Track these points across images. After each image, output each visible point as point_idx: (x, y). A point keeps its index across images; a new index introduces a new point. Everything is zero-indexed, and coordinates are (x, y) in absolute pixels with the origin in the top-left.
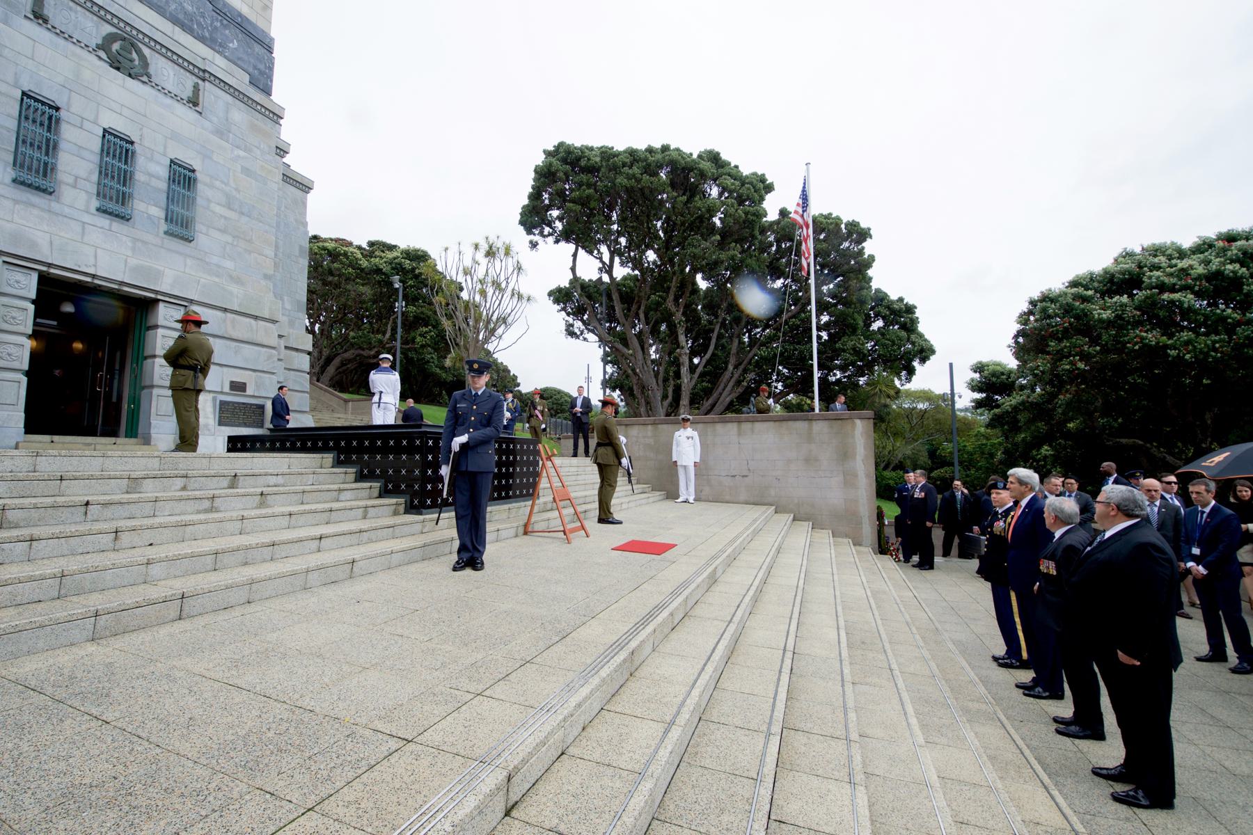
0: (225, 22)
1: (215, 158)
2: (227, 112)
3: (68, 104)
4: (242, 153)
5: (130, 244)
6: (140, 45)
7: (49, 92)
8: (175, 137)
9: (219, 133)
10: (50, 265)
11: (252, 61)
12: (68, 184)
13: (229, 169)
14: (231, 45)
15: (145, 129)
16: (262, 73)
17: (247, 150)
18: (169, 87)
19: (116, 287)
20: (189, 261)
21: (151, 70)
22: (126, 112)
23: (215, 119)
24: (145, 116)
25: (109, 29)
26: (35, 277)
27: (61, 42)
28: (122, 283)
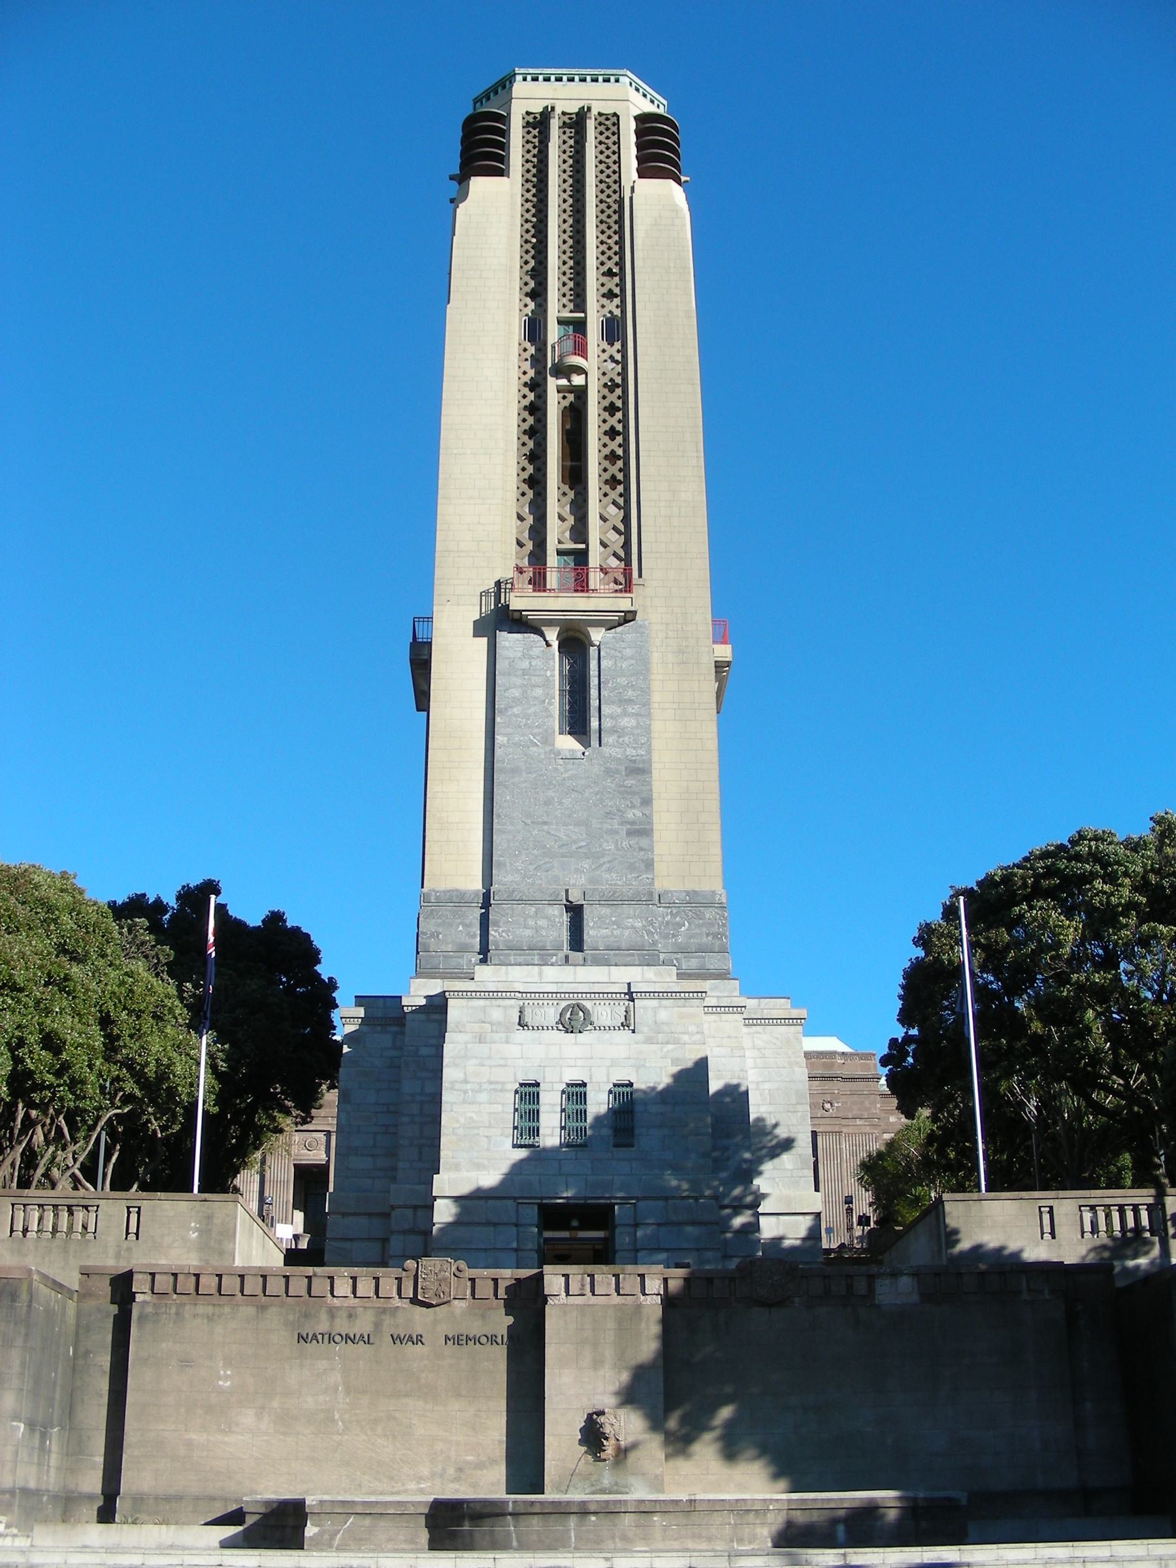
0: (675, 911)
1: (647, 1065)
2: (655, 1016)
3: (544, 1078)
4: (670, 1047)
5: (590, 1165)
6: (584, 1003)
7: (531, 1077)
8: (615, 1063)
9: (649, 1041)
10: (542, 1198)
11: (704, 930)
12: (549, 1136)
13: (661, 1068)
14: (682, 929)
15: (593, 1069)
16: (715, 936)
17: (676, 1042)
18: (608, 1023)
19: (582, 1202)
20: (634, 1165)
21: (594, 1018)
22: (579, 1063)
23: (645, 1029)
24: (592, 1058)
25: (564, 1004)
26: (536, 1207)
27: (536, 1034)
28: (586, 1198)
